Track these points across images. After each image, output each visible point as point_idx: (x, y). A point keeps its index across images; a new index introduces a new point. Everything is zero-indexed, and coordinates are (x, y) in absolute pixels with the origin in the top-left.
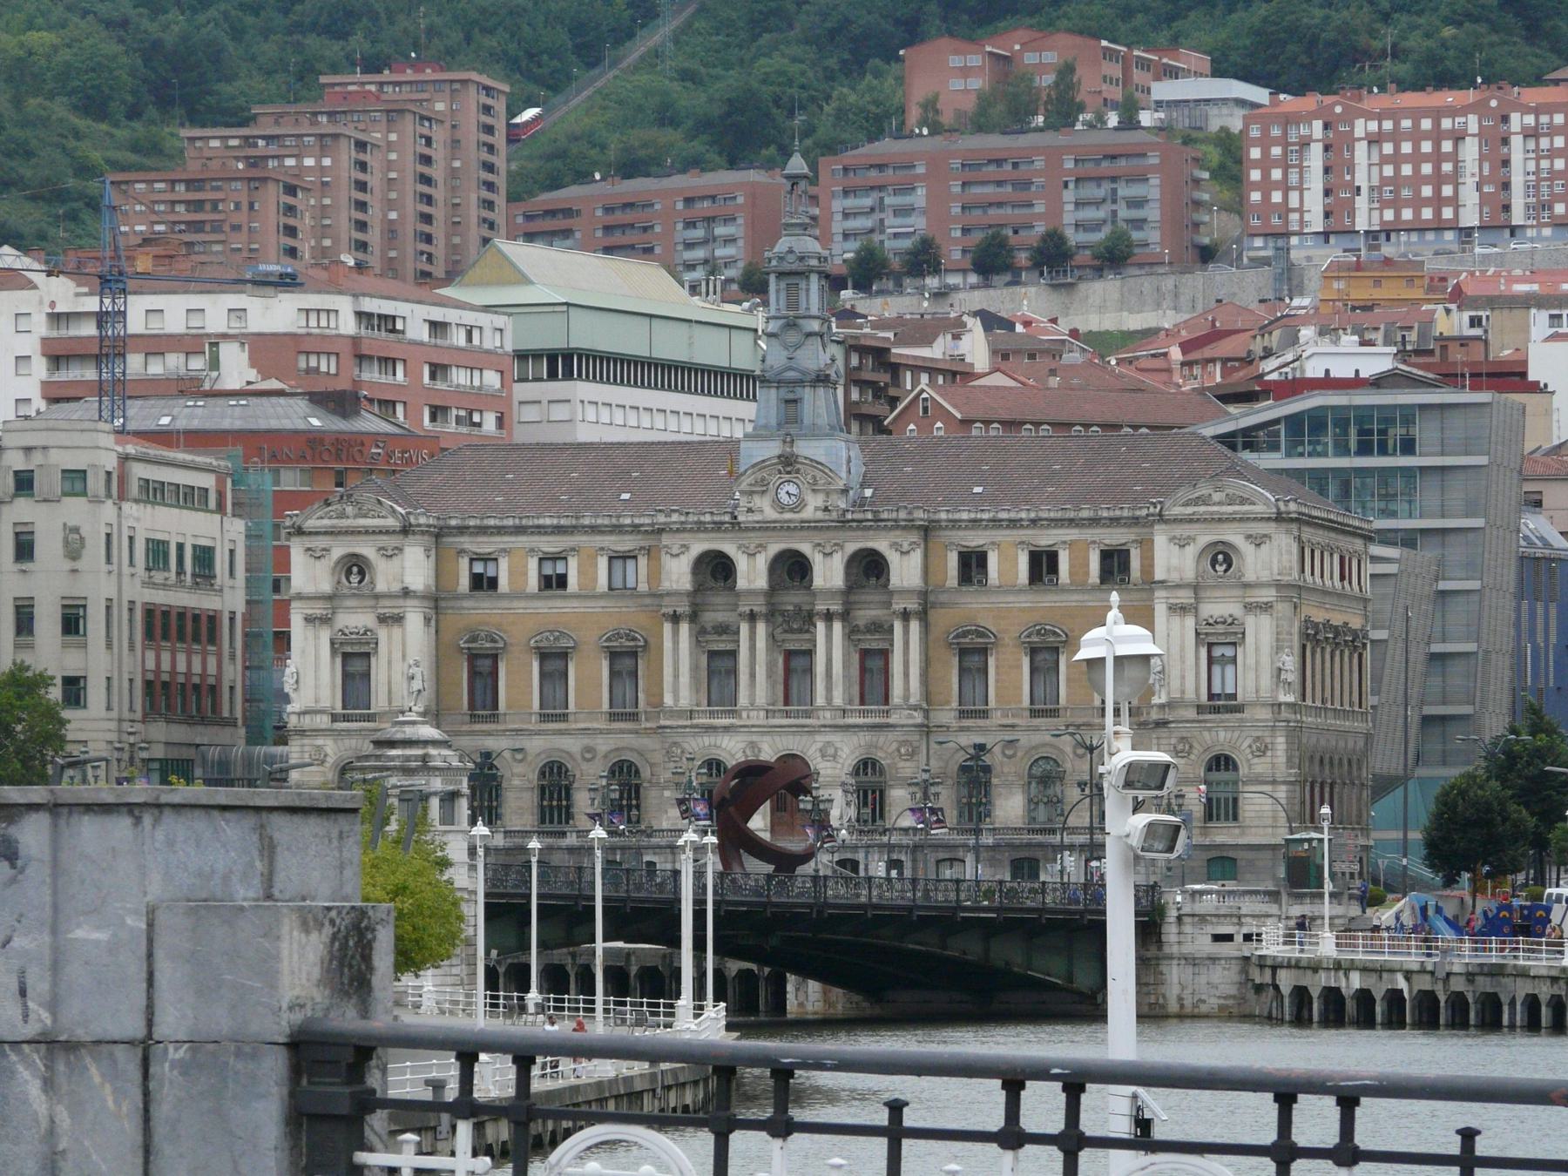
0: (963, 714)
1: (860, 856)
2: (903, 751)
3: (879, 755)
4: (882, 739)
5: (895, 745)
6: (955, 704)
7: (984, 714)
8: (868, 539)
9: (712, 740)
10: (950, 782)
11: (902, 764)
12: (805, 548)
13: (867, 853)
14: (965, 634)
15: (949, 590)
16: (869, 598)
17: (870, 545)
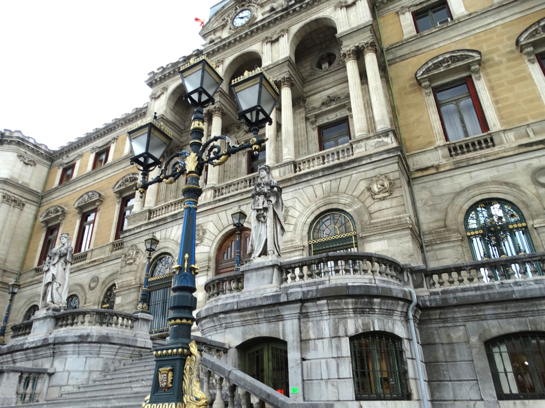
0: (454, 150)
1: (288, 329)
2: (375, 188)
3: (343, 202)
4: (344, 182)
5: (363, 185)
6: (441, 141)
7: (489, 142)
8: (310, 15)
9: (163, 232)
10: (454, 237)
11: (377, 206)
12: (256, 47)
13: (303, 315)
14: (437, 66)
15: (408, 42)
16: (323, 82)
17: (314, 17)
